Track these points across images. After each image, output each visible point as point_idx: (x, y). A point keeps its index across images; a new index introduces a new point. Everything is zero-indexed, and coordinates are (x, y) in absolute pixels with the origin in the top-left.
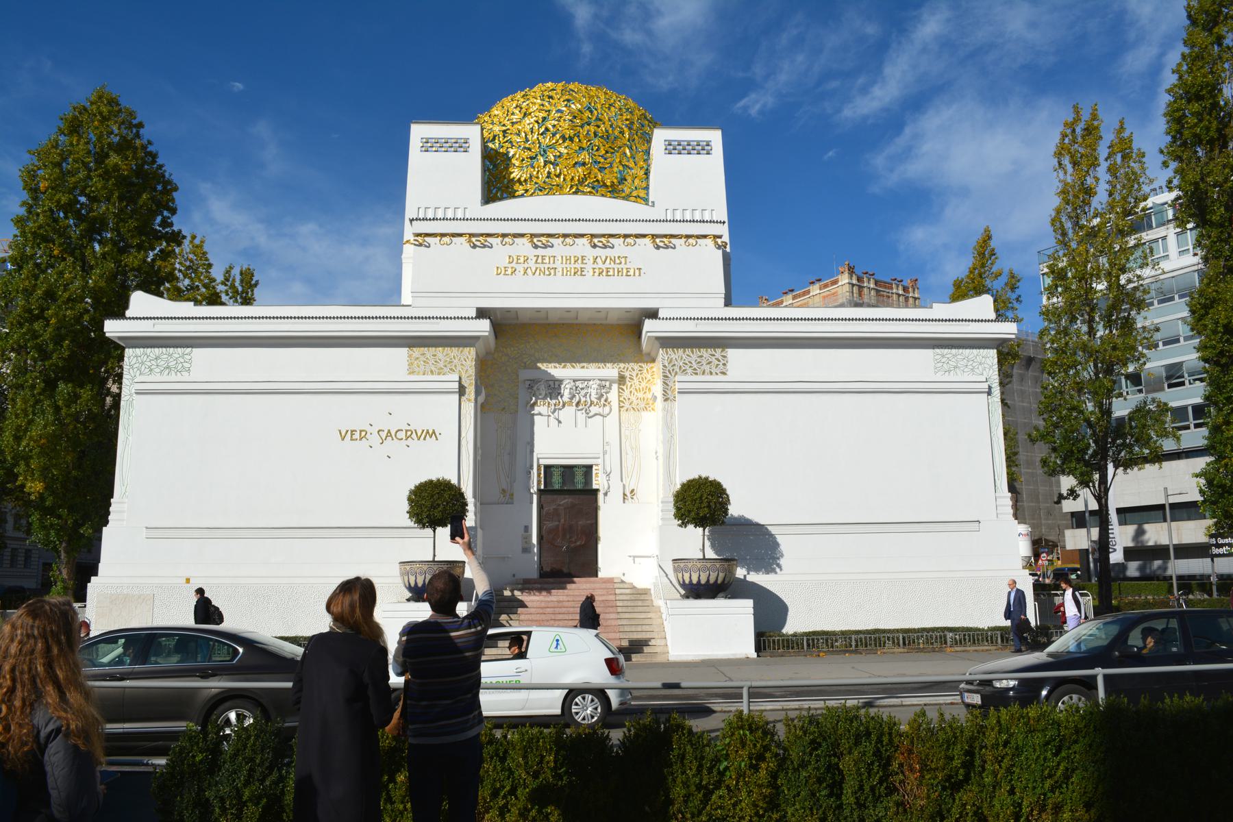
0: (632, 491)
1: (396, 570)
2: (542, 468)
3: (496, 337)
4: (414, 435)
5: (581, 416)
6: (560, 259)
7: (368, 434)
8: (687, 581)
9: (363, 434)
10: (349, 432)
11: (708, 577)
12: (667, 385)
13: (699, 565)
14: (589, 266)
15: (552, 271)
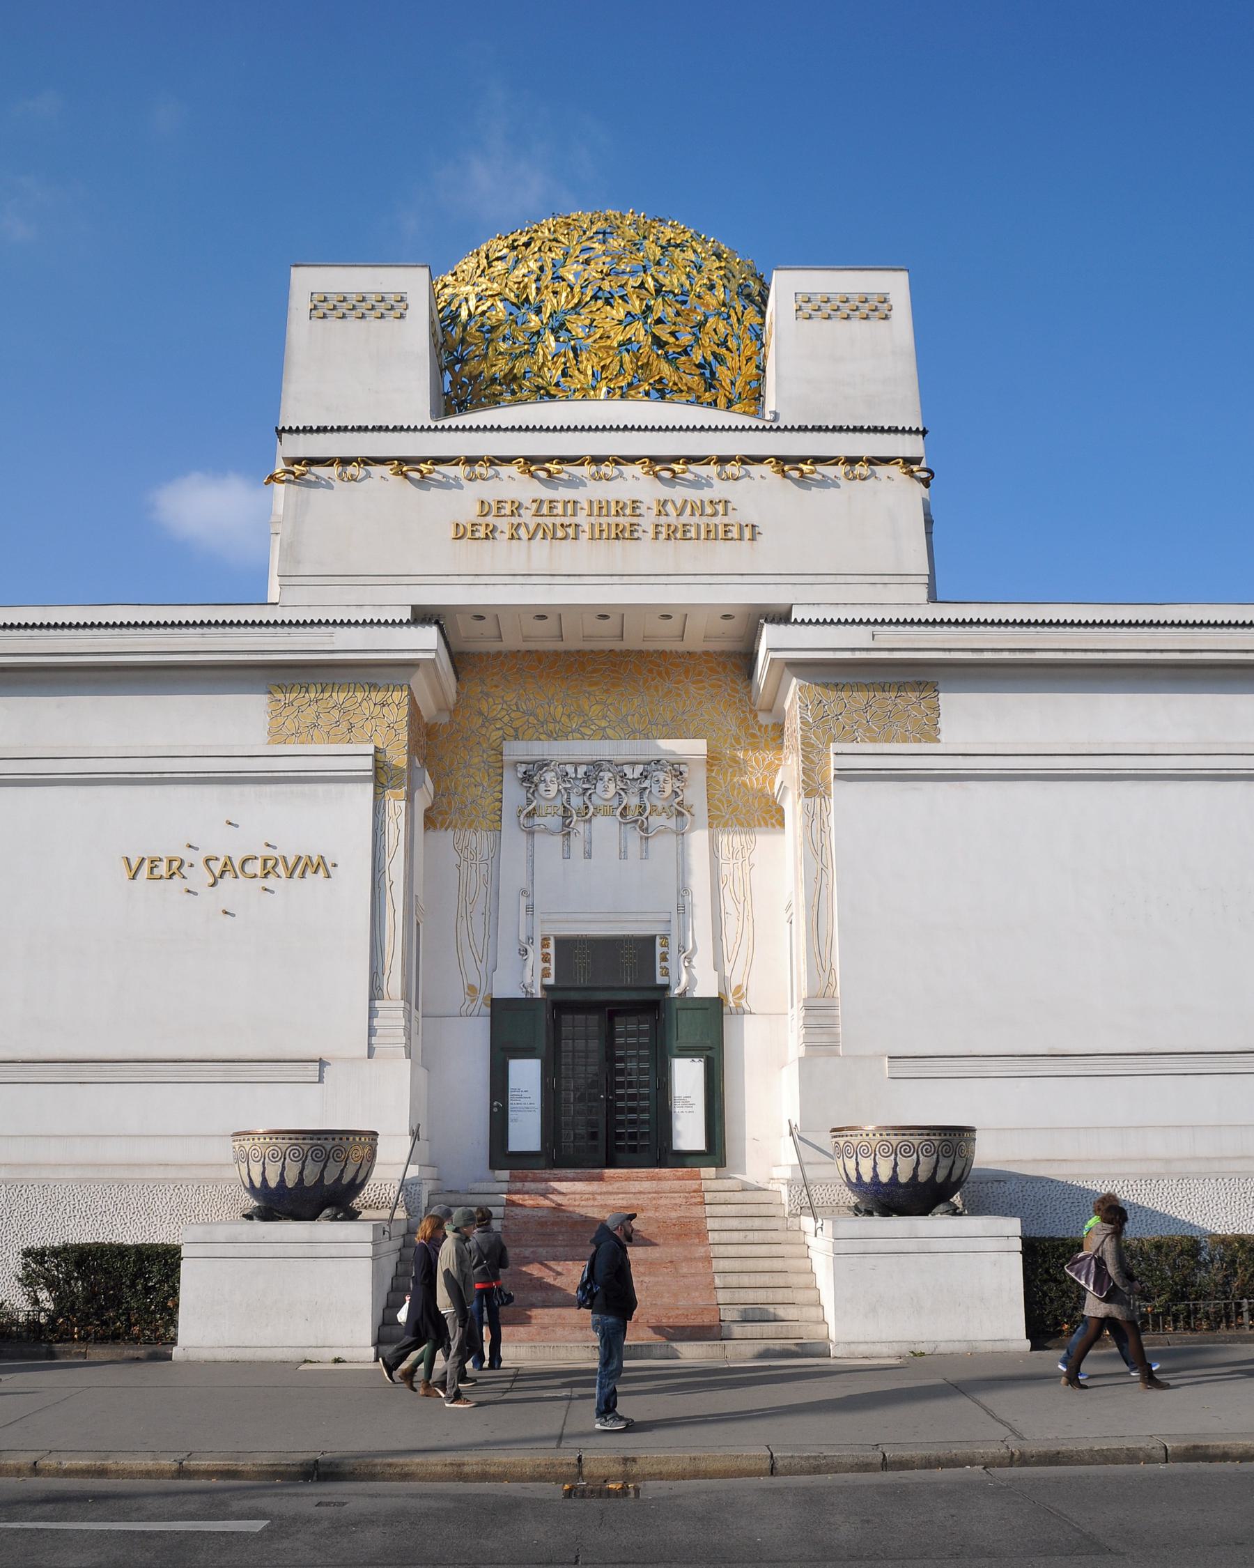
0: (739, 988)
1: (223, 1151)
2: (552, 942)
3: (458, 679)
4: (280, 869)
5: (634, 836)
6: (586, 506)
7: (186, 865)
8: (867, 1178)
9: (175, 865)
10: (146, 865)
11: (916, 1169)
12: (812, 762)
13: (895, 1140)
14: (647, 522)
15: (571, 531)
